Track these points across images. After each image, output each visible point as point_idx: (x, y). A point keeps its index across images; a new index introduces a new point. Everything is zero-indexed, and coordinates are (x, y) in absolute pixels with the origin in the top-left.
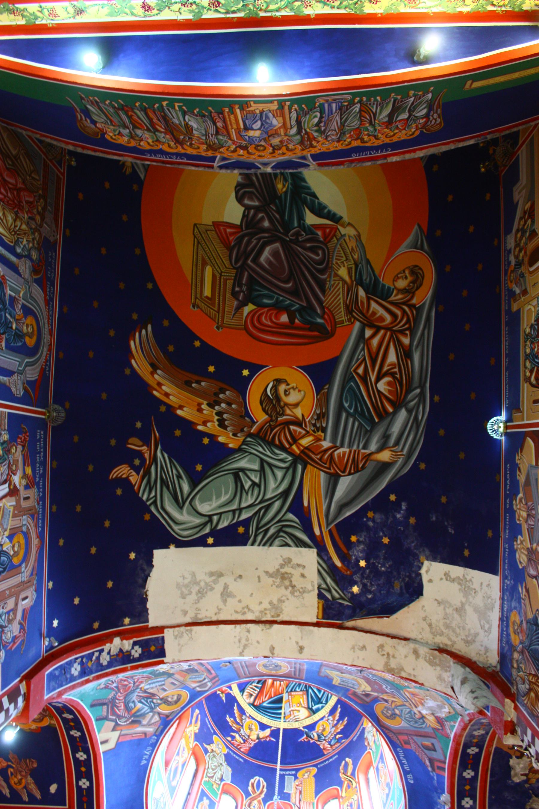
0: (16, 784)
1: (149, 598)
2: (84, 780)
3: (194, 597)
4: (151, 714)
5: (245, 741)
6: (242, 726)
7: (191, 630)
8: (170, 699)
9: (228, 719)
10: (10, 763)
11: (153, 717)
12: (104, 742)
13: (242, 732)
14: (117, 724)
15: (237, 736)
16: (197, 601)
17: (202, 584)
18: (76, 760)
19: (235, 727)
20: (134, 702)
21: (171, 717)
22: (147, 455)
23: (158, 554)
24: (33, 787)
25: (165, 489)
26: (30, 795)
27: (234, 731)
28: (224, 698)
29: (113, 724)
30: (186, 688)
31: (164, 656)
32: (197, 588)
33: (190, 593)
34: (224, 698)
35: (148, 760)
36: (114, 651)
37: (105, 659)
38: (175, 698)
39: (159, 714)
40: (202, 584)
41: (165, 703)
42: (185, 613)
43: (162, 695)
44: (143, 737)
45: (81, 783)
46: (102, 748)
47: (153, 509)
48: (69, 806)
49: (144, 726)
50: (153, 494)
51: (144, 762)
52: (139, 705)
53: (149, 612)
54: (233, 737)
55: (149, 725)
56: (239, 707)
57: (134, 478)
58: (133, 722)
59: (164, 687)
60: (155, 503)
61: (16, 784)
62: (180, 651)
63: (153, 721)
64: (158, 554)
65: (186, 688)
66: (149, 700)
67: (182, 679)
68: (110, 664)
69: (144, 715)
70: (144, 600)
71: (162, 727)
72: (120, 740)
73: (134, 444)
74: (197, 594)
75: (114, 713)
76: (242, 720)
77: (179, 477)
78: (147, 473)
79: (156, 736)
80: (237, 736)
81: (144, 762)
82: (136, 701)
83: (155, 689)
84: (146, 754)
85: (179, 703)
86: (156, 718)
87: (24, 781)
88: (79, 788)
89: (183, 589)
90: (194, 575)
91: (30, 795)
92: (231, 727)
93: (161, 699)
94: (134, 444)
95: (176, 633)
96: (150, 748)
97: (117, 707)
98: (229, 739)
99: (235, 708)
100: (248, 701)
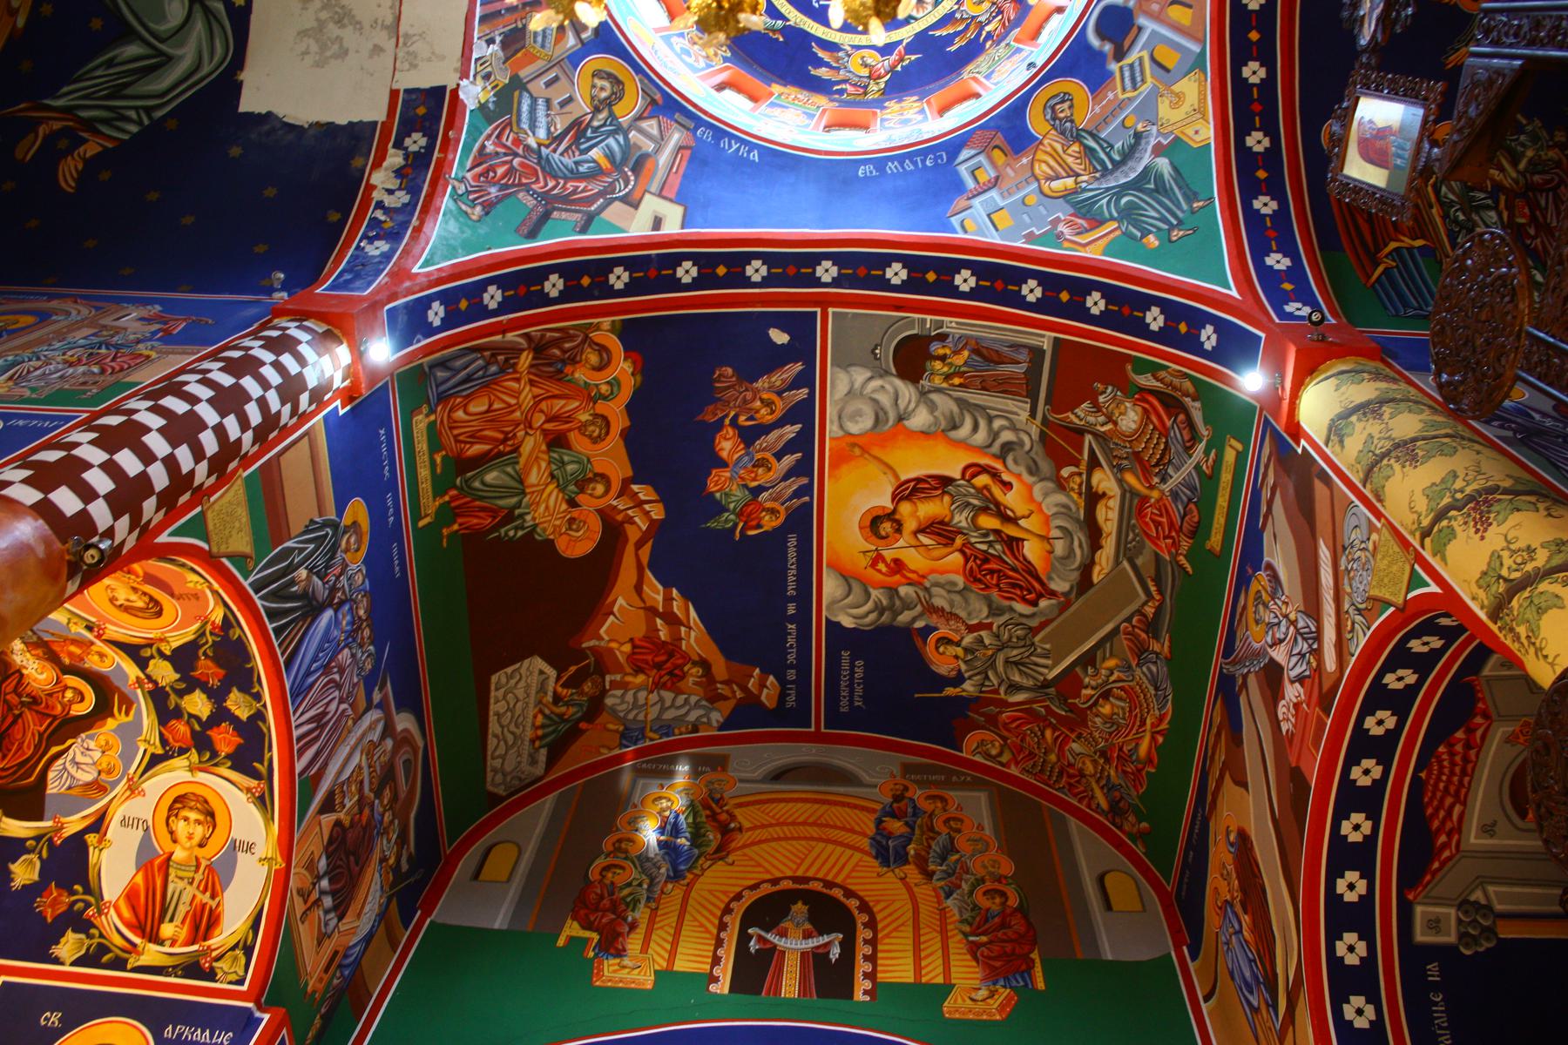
0: (773, 412)
1: (330, 120)
2: (749, 271)
3: (348, 34)
4: (632, 134)
5: (1000, 12)
6: (973, 18)
7: (407, 36)
8: (604, 95)
9: (953, 48)
10: (727, 421)
11: (641, 131)
12: (657, 223)
13: (983, 19)
14: (624, 200)
15: (988, 28)
16: (358, 26)
17: (324, 15)
18: (696, 284)
19: (971, 34)
20: (577, 163)
21: (658, 96)
22: (57, 125)
23: (251, 102)
24: (778, 378)
25: (128, 91)
26: (795, 384)
27: (979, 34)
28: (913, 57)
29: (617, 206)
30: (575, 59)
31: (444, 88)
32: (331, 25)
33: (339, 39)
34: (913, 57)
35: (752, 147)
36: (393, 183)
37: (403, 198)
38: (599, 83)
39: (640, 118)
40: (324, 15)
41: (610, 105)
42: (377, 50)
43: (582, 106)
44: (687, 153)
45: (756, 278)
46: (672, 226)
47: (159, 114)
48: (816, 304)
49: (657, 151)
50: (133, 114)
51: (755, 156)
52: (595, 153)
53: (355, 120)
54: (989, 36)
55: (661, 141)
56: (935, 26)
57: (91, 149)
58: (636, 169)
59: (556, 102)
60: (148, 110)
61: (773, 412)
62: (443, 58)
63: (655, 132)
64: (251, 102)
65: (575, 59)
66: (589, 133)
67: (540, 64)
68: (414, 191)
69: (627, 148)
70: (330, 129)
71: (677, 116)
72: (673, 196)
73: (28, 149)
74: (343, 26)
75: (590, 200)
76: (962, 19)
77: (110, 63)
78: (89, 125)
79: (696, 129)
80: (988, 28)
81: (755, 156)
82: (577, 158)
83: (558, 120)
84: (738, 149)
85: (621, 77)
86: (651, 126)
87: (765, 396)
88: (765, 282)
89: (328, 54)
90: (303, 33)
91: (795, 384)
92: (970, 42)
93: (597, 110)
94: (28, 149)
95: (406, 66)
96: (724, 143)
97: (574, 192)
98: (988, 44)
99: (938, 33)
100: (930, 8)
